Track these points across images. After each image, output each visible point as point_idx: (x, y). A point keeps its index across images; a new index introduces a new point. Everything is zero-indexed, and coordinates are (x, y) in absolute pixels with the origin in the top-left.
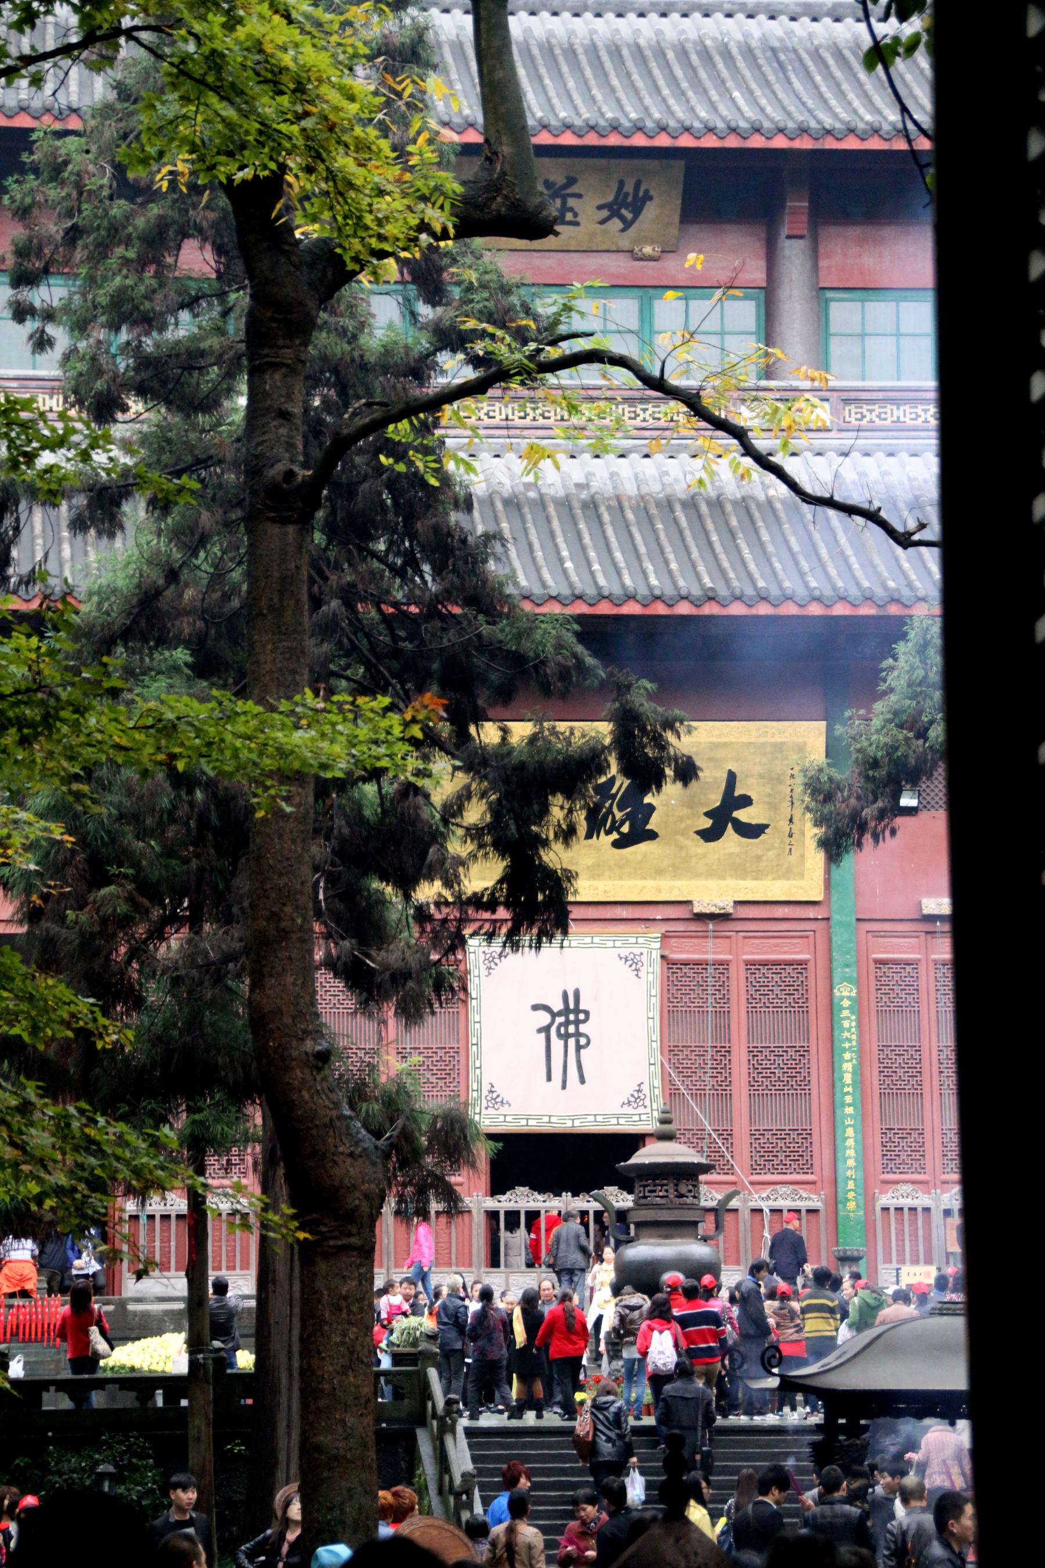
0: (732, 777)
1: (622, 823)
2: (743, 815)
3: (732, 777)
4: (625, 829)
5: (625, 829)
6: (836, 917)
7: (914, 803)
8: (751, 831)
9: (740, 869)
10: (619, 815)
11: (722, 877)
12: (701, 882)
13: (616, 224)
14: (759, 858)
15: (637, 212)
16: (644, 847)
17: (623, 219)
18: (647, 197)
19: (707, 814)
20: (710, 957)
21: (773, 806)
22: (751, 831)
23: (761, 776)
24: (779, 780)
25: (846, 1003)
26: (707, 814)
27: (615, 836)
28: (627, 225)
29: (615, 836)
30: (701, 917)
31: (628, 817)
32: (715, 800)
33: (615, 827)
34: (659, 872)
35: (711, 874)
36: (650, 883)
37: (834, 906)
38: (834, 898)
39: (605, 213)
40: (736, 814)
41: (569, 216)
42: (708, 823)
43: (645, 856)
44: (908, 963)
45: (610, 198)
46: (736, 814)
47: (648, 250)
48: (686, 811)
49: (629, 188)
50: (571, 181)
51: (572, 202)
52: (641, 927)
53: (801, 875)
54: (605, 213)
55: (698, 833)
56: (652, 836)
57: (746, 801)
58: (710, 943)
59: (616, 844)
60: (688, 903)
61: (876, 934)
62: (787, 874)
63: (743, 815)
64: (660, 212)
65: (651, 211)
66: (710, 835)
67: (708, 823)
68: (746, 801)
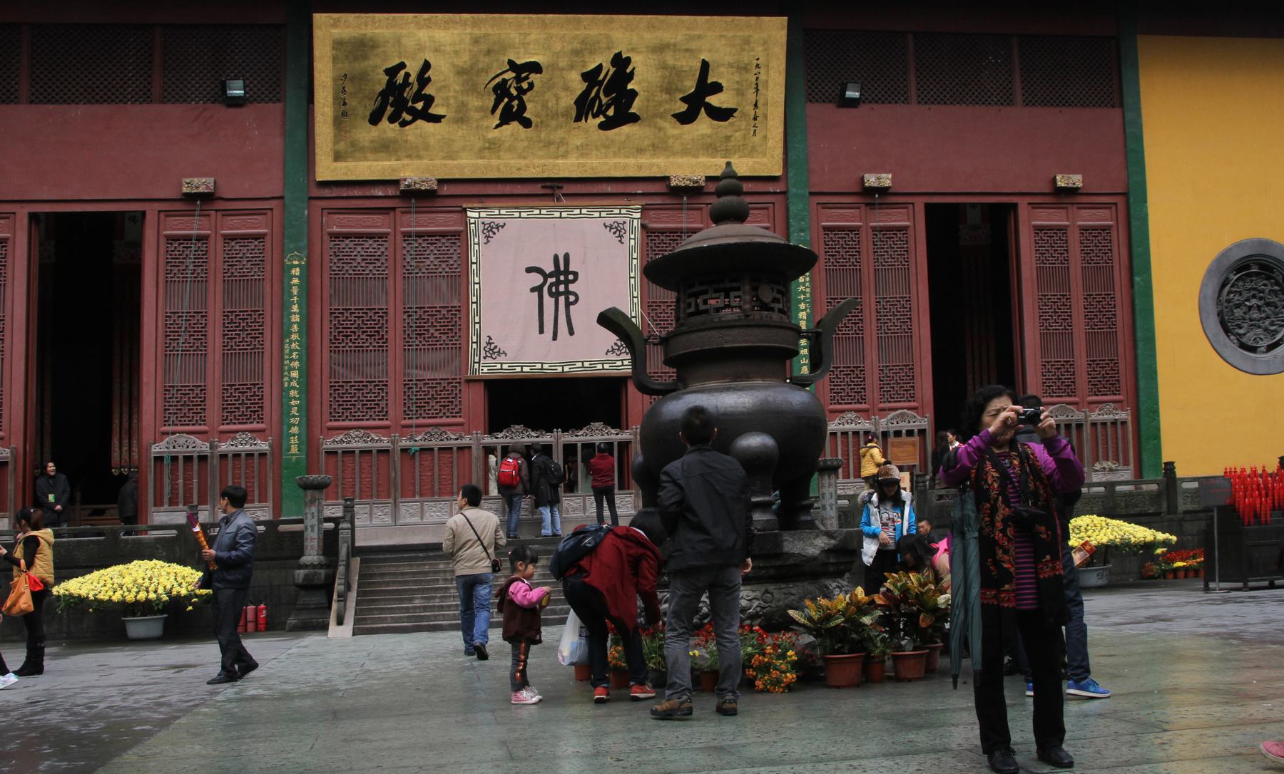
1: (608, 107)
2: (714, 100)
3: (705, 66)
4: (611, 112)
5: (611, 112)
6: (792, 190)
7: (857, 95)
8: (721, 115)
9: (710, 148)
10: (604, 100)
11: (696, 156)
12: (679, 160)
14: (728, 138)
16: (626, 129)
19: (683, 99)
20: (684, 225)
21: (740, 93)
22: (721, 115)
23: (730, 65)
24: (746, 69)
26: (683, 99)
27: (602, 119)
29: (602, 119)
30: (678, 192)
31: (613, 102)
32: (690, 86)
33: (602, 111)
34: (640, 151)
35: (685, 152)
36: (632, 161)
37: (791, 181)
38: (791, 174)
40: (708, 99)
42: (683, 107)
43: (628, 136)
44: (851, 229)
46: (708, 99)
48: (665, 96)
52: (625, 201)
53: (764, 154)
55: (675, 116)
56: (635, 119)
57: (717, 88)
58: (685, 214)
59: (603, 126)
60: (667, 179)
61: (825, 206)
62: (752, 152)
63: (714, 100)
66: (685, 118)
67: (683, 107)
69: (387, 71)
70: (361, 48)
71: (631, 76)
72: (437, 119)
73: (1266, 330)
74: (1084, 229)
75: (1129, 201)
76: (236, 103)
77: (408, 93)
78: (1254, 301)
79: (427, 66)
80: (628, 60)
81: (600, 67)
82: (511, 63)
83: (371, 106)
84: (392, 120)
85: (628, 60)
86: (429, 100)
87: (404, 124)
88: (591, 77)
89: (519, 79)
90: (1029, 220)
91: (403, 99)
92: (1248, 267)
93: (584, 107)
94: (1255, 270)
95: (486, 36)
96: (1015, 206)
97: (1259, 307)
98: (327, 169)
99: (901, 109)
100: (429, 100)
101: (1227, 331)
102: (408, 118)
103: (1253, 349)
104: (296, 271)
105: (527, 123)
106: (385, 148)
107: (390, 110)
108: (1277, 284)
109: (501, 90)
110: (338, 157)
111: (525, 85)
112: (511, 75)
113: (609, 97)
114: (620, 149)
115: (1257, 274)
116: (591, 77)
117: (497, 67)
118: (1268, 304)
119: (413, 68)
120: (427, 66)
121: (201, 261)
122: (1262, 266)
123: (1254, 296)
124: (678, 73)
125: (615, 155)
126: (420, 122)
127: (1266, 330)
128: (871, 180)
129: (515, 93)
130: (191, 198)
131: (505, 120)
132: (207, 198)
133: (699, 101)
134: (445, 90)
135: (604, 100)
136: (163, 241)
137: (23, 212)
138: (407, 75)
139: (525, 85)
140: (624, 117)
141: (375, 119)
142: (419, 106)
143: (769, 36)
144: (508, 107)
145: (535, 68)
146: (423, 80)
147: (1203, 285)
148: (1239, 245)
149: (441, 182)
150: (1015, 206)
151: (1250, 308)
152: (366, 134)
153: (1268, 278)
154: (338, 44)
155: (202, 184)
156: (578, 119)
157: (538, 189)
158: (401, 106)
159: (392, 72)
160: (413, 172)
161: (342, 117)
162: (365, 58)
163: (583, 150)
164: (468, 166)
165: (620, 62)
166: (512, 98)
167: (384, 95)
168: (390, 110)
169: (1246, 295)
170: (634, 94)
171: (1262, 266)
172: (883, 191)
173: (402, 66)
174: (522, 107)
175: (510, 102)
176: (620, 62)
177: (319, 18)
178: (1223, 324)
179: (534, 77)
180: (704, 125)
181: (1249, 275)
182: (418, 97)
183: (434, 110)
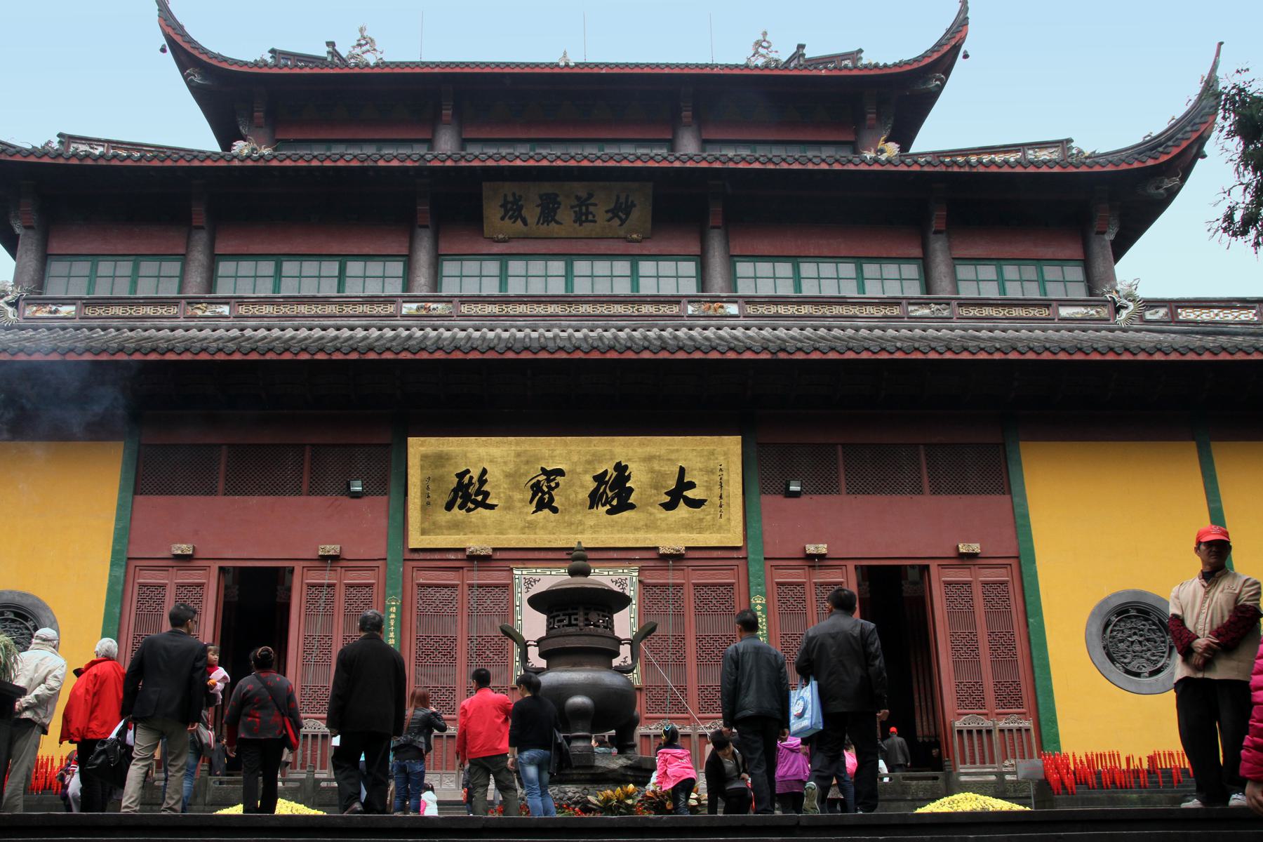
0: (682, 471)
2: (689, 494)
3: (682, 470)
4: (615, 503)
5: (615, 503)
6: (751, 557)
7: (798, 489)
8: (695, 504)
9: (688, 526)
10: (610, 494)
11: (678, 532)
12: (665, 535)
13: (617, 222)
14: (701, 520)
15: (628, 214)
16: (625, 514)
17: (620, 218)
18: (633, 205)
19: (667, 493)
20: (670, 581)
21: (709, 488)
22: (695, 504)
23: (701, 470)
24: (712, 472)
25: (759, 607)
26: (667, 493)
27: (608, 507)
28: (623, 222)
29: (608, 507)
30: (665, 557)
31: (616, 495)
32: (672, 484)
34: (637, 529)
35: (670, 530)
36: (631, 536)
37: (750, 550)
38: (750, 545)
39: (610, 215)
41: (590, 217)
42: (668, 499)
43: (628, 519)
44: (798, 584)
45: (612, 206)
47: (635, 236)
48: (654, 491)
49: (622, 200)
50: (590, 196)
51: (591, 209)
52: (627, 564)
53: (729, 531)
54: (610, 215)
56: (632, 507)
57: (692, 485)
58: (671, 573)
59: (609, 512)
60: (656, 548)
61: (777, 567)
62: (720, 529)
63: (689, 494)
64: (640, 214)
65: (635, 214)
66: (669, 506)
67: (668, 499)
68: (692, 485)
69: (458, 475)
70: (440, 460)
71: (628, 478)
72: (492, 507)
73: (1148, 659)
74: (985, 583)
75: (1020, 562)
76: (356, 495)
77: (472, 490)
78: (1135, 638)
79: (484, 472)
80: (626, 467)
81: (606, 472)
82: (543, 469)
83: (446, 499)
84: (461, 508)
85: (626, 467)
86: (486, 494)
87: (469, 510)
88: (600, 479)
89: (549, 481)
90: (939, 579)
91: (468, 493)
92: (1127, 611)
93: (595, 499)
94: (1133, 613)
95: (525, 451)
96: (927, 567)
97: (1140, 642)
98: (416, 540)
99: (833, 499)
100: (486, 494)
101: (1113, 660)
102: (472, 506)
103: (1138, 675)
104: (393, 609)
105: (555, 510)
106: (456, 526)
107: (459, 501)
108: (1154, 624)
109: (536, 488)
110: (423, 532)
111: (553, 484)
112: (543, 478)
113: (614, 492)
114: (623, 528)
115: (1135, 617)
116: (600, 479)
117: (534, 472)
118: (1148, 640)
119: (475, 473)
120: (484, 472)
121: (330, 601)
122: (1139, 611)
123: (1135, 634)
124: (663, 475)
125: (619, 531)
126: (480, 509)
127: (1148, 659)
128: (811, 549)
129: (546, 489)
130: (324, 558)
131: (539, 507)
132: (335, 558)
133: (678, 493)
134: (497, 487)
135: (610, 494)
136: (305, 587)
137: (215, 566)
138: (471, 478)
139: (553, 484)
140: (624, 505)
141: (449, 507)
142: (480, 498)
143: (729, 449)
144: (542, 499)
145: (560, 472)
146: (482, 481)
147: (1088, 625)
148: (1115, 595)
149: (495, 550)
150: (927, 567)
151: (1132, 642)
152: (444, 517)
153: (1146, 620)
154: (424, 457)
155: (331, 549)
156: (591, 507)
157: (563, 555)
158: (467, 498)
159: (461, 476)
160: (476, 543)
161: (427, 505)
162: (443, 466)
163: (595, 529)
164: (513, 539)
165: (621, 468)
166: (544, 493)
167: (455, 491)
168: (459, 501)
169: (1128, 632)
170: (631, 490)
171: (1139, 611)
172: (822, 557)
173: (468, 471)
174: (552, 499)
175: (542, 497)
176: (621, 468)
177: (412, 441)
178: (1109, 655)
179: (559, 479)
180: (683, 511)
181: (1129, 617)
182: (478, 492)
183: (488, 502)
